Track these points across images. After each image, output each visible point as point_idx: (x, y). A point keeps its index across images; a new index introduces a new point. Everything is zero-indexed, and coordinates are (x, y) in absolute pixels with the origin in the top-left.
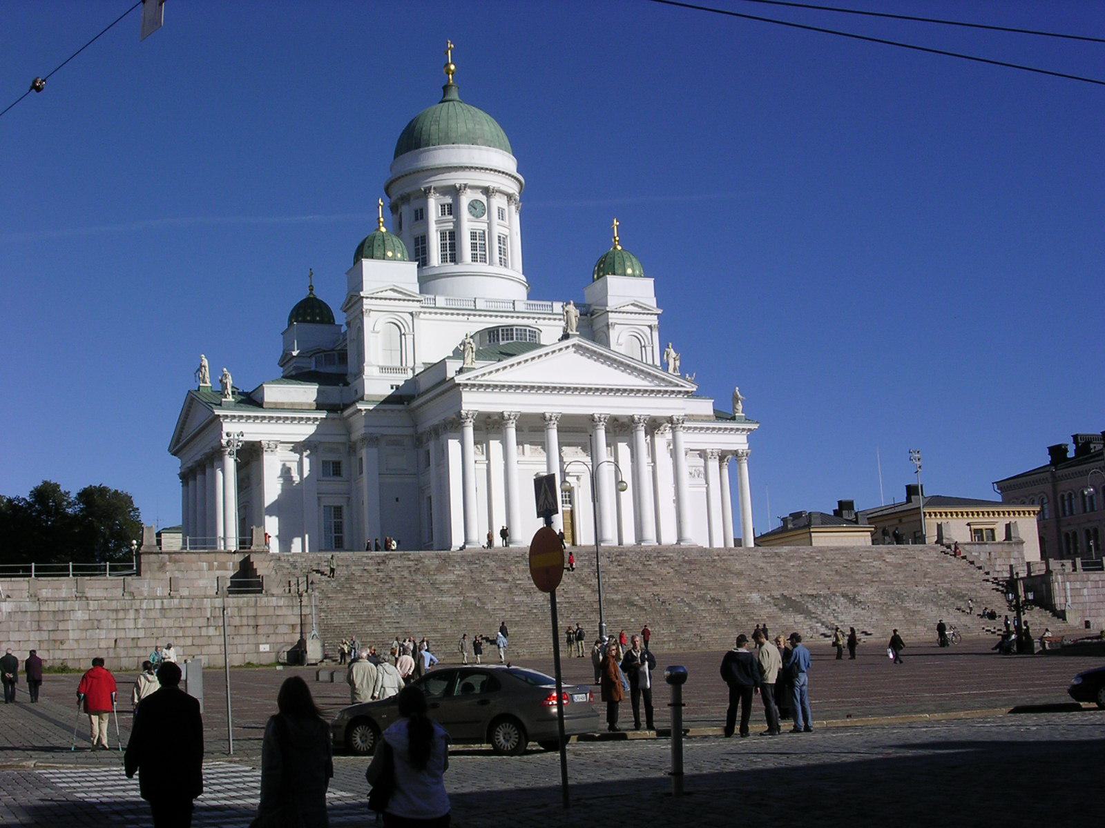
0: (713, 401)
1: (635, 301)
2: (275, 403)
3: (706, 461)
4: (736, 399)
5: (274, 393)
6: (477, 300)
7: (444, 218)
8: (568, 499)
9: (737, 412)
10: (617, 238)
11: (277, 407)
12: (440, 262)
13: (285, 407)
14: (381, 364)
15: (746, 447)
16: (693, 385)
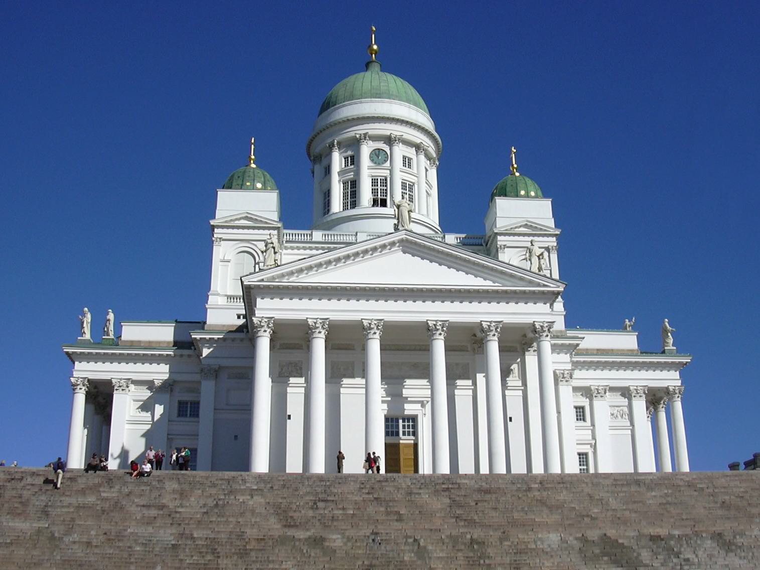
0: (637, 333)
1: (528, 221)
2: (132, 342)
3: (630, 400)
4: (666, 331)
5: (132, 332)
6: (358, 234)
7: (347, 168)
8: (411, 430)
9: (667, 346)
10: (515, 166)
11: (132, 345)
12: (342, 210)
13: (142, 345)
14: (228, 294)
15: (679, 383)
16: (559, 284)
